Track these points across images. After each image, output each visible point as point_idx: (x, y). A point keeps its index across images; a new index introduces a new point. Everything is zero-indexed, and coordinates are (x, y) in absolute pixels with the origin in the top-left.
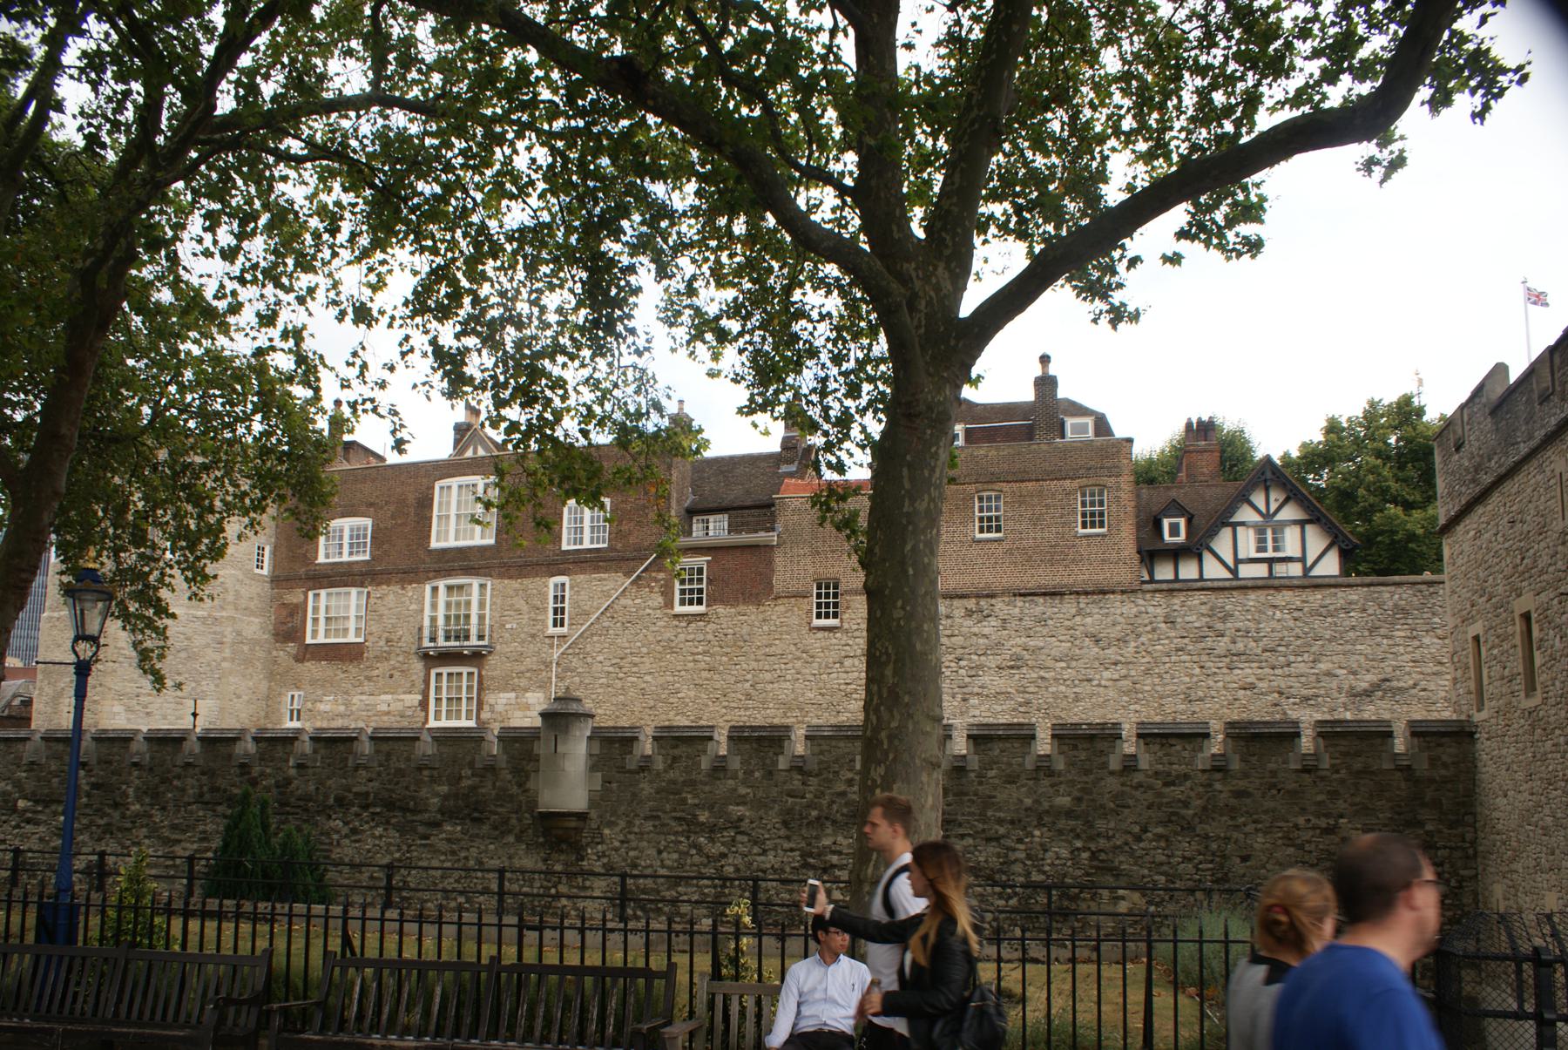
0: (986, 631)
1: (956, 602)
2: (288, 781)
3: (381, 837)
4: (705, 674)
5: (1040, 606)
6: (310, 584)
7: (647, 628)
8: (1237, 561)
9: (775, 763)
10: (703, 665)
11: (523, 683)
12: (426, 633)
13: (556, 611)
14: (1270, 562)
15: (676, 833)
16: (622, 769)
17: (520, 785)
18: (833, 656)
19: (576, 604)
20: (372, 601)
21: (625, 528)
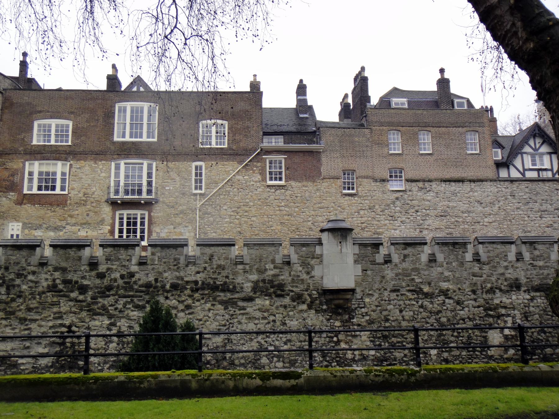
0: (429, 198)
1: (414, 184)
2: (132, 275)
3: (209, 310)
4: (286, 217)
5: (454, 187)
6: (28, 157)
7: (252, 192)
8: (525, 170)
9: (463, 257)
10: (285, 213)
11: (178, 220)
12: (112, 190)
13: (196, 181)
14: (539, 170)
15: (410, 300)
16: (374, 263)
17: (308, 273)
18: (354, 209)
19: (208, 177)
20: (73, 170)
21: (237, 137)
